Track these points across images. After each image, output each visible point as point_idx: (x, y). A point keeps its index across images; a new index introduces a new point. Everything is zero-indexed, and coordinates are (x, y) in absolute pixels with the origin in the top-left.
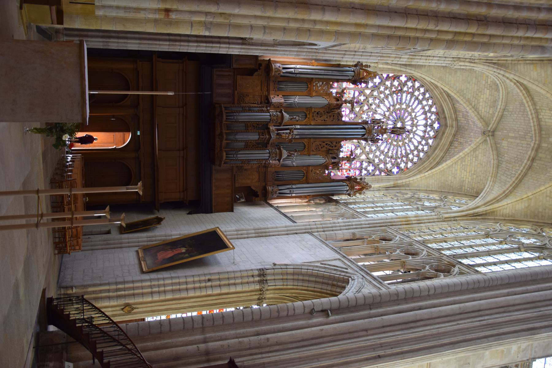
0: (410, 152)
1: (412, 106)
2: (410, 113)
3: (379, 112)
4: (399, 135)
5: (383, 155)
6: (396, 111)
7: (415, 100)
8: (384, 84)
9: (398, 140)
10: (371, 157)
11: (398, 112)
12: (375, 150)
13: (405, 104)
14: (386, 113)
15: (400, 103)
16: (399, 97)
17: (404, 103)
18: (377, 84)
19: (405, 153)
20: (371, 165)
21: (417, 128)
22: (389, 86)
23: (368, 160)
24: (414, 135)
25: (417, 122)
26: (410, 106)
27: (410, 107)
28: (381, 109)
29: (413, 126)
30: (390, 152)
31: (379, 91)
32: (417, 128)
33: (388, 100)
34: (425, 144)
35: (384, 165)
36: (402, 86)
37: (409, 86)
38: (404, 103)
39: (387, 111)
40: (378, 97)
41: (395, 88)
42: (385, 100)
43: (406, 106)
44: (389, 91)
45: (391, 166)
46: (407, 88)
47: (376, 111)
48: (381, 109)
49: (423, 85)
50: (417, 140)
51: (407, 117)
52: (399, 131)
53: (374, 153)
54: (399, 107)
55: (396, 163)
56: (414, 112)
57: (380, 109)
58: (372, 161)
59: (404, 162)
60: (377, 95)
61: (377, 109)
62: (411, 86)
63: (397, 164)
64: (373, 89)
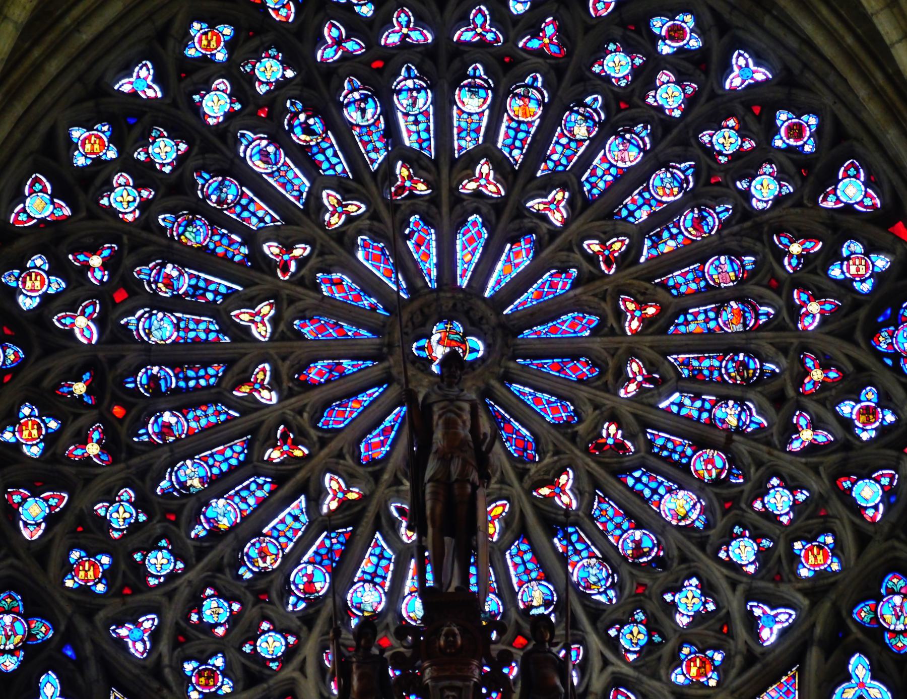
0: (719, 199)
1: (251, 239)
2: (320, 251)
3: (322, 584)
4: (483, 462)
5: (762, 492)
6: (314, 396)
7: (199, 208)
8: (41, 549)
9: (598, 344)
10: (785, 616)
11: (316, 372)
12: (707, 589)
13: (243, 317)
14: (330, 504)
15: (229, 364)
16: (169, 378)
17: (228, 326)
18: (42, 630)
19: (735, 254)
20: (863, 613)
21: (471, 159)
22: (60, 500)
23: (814, 656)
24: (553, 181)
25: (412, 159)
26: (257, 258)
27: (271, 249)
28: (291, 560)
29: (457, 199)
30: (729, 414)
31: (114, 607)
32: (471, 159)
33: (203, 500)
34: (629, 51)
35: (866, 474)
36: (60, 363)
37: (56, 285)
38: (228, 326)
39: (316, 496)
40: (171, 616)
41: (84, 441)
42: (199, 531)
43: (251, 302)
44: (111, 498)
45: (870, 396)
46: (72, 307)
47: (307, 619)
48: (291, 560)
49: (35, 142)
50: (597, 144)
51: (369, 284)
52: (445, 459)
53: (734, 602)
54: (264, 372)
55: (837, 348)
56: (314, 206)
57: (298, 577)
58: (827, 605)
59: (833, 255)
60: (148, 622)
61: (295, 604)
62: (57, 268)
63: (847, 335)
64: (93, 670)
